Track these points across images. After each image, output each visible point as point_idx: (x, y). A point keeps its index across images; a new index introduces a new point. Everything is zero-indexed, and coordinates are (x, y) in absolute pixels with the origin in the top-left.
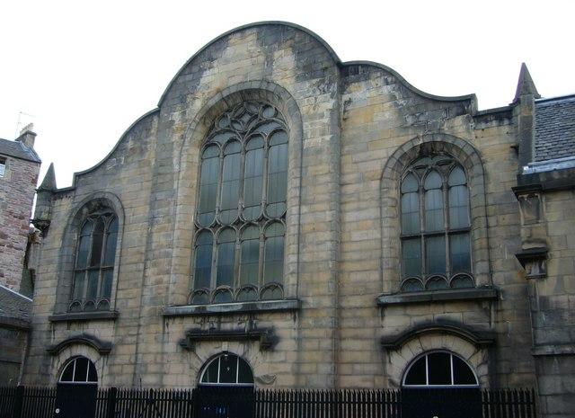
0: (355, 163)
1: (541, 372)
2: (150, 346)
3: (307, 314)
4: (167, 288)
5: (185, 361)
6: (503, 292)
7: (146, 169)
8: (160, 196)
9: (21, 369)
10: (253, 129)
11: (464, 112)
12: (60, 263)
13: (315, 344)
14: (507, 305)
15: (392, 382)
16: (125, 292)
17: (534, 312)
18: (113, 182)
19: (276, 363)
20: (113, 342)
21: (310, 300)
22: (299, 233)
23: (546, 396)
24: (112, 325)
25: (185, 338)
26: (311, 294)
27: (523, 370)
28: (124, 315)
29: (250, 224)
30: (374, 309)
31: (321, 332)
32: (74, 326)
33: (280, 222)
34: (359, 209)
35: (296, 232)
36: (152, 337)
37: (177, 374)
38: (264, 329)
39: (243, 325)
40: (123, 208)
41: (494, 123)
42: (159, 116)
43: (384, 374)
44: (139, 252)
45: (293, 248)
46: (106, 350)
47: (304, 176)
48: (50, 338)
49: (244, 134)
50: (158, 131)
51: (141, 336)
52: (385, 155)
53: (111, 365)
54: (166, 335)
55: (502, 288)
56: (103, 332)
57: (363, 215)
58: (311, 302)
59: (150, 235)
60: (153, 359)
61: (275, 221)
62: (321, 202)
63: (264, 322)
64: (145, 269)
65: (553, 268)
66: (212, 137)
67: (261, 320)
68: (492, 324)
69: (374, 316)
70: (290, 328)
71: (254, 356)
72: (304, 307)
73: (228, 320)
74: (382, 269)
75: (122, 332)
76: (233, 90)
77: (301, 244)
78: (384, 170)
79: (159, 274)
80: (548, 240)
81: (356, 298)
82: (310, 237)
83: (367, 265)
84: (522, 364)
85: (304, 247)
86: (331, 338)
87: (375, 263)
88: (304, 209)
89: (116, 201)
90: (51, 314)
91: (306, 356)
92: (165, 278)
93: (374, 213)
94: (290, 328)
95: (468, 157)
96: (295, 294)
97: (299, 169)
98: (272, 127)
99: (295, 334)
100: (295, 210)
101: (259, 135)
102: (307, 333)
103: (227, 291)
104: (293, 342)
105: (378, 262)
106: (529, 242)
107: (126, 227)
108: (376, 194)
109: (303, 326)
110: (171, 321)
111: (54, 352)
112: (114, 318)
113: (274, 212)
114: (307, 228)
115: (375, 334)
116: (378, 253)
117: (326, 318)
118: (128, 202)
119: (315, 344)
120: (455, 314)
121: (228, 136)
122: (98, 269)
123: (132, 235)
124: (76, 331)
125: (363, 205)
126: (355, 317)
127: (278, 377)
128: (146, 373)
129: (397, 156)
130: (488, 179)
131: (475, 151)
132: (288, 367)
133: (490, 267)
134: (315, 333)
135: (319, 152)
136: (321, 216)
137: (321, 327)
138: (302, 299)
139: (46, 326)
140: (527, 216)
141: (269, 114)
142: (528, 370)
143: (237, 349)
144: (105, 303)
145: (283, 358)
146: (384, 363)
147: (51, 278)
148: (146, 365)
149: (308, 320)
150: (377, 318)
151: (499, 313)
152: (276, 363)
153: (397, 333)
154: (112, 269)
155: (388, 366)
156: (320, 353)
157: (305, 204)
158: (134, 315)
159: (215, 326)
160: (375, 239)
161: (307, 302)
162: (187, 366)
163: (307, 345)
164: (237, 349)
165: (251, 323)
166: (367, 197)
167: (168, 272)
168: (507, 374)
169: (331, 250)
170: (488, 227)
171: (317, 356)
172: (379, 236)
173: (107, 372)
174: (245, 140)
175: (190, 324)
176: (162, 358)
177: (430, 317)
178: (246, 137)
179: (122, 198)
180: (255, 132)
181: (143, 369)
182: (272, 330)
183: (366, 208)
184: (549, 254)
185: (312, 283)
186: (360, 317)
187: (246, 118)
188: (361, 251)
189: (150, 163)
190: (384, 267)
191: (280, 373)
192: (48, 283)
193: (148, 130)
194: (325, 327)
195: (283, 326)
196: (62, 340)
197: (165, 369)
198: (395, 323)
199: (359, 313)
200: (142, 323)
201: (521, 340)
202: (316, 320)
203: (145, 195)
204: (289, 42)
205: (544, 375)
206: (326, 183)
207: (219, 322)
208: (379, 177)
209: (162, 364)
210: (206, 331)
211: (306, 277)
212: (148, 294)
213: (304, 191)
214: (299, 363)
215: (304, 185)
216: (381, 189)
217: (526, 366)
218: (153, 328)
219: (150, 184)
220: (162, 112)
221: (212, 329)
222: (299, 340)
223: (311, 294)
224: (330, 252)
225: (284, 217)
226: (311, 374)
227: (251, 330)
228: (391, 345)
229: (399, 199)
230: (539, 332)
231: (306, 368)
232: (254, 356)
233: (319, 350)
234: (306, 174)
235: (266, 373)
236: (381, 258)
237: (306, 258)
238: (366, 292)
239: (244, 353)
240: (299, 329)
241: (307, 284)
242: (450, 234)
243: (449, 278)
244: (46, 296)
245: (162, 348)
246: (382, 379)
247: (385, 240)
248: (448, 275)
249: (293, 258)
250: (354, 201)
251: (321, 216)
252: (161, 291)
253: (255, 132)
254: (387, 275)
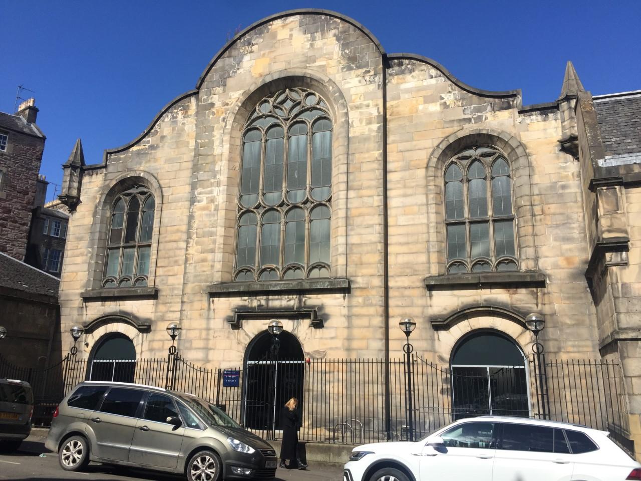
0: (401, 152)
1: (626, 355)
3: (355, 293)
4: (212, 266)
5: (232, 336)
6: (549, 276)
7: (184, 150)
8: (202, 175)
9: (50, 345)
10: (296, 116)
11: (509, 107)
12: (92, 240)
13: (364, 322)
14: (552, 287)
15: (442, 359)
16: (165, 269)
17: (615, 298)
18: (149, 161)
19: (326, 339)
20: (153, 318)
21: (359, 279)
22: (347, 217)
23: (631, 377)
24: (151, 302)
25: (232, 314)
26: (360, 274)
27: (571, 349)
28: (164, 292)
29: (295, 207)
30: (421, 289)
31: (372, 310)
32: (108, 303)
33: (326, 205)
34: (405, 196)
35: (344, 215)
36: (196, 314)
37: (224, 350)
38: (314, 307)
39: (292, 303)
40: (160, 187)
41: (539, 117)
42: (197, 99)
43: (433, 351)
44: (178, 231)
45: (342, 230)
46: (145, 328)
47: (350, 162)
48: (82, 315)
49: (287, 119)
50: (197, 113)
51: (184, 312)
52: (431, 146)
53: (150, 341)
54: (212, 312)
55: (548, 272)
56: (141, 308)
57: (409, 201)
58: (360, 281)
59: (191, 217)
60: (198, 335)
61: (321, 204)
62: (369, 187)
63: (313, 300)
64: (187, 247)
65: (633, 256)
66: (251, 123)
67: (310, 298)
68: (540, 305)
69: (424, 296)
70: (340, 306)
71: (302, 330)
72: (352, 286)
73: (276, 297)
74: (429, 252)
75: (162, 308)
76: (276, 77)
77: (349, 228)
78: (430, 159)
79: (202, 252)
80: (629, 230)
81: (403, 278)
82: (358, 221)
83: (414, 248)
84: (570, 343)
85: (352, 230)
86: (382, 316)
87: (421, 247)
88: (352, 194)
89: (153, 180)
90: (83, 291)
91: (356, 332)
92: (210, 256)
93: (422, 199)
94: (340, 306)
95: (513, 149)
96: (345, 275)
97: (346, 156)
98: (317, 114)
99: (345, 311)
100: (342, 194)
101: (303, 122)
102: (355, 310)
103: (273, 270)
104: (344, 319)
105: (425, 245)
106: (609, 231)
107: (164, 206)
108: (423, 182)
109: (354, 304)
110: (216, 299)
111: (89, 328)
112: (154, 295)
113: (319, 195)
114: (353, 212)
115: (423, 312)
116: (425, 236)
117: (376, 297)
118: (167, 181)
119: (364, 322)
121: (271, 121)
123: (170, 217)
124: (111, 307)
125: (409, 191)
126: (403, 296)
127: (328, 352)
128: (190, 349)
129: (443, 146)
130: (533, 170)
131: (521, 144)
132: (339, 343)
133: (536, 252)
134: (364, 311)
135: (366, 139)
136: (369, 201)
137: (371, 305)
138: (352, 279)
139: (77, 301)
140: (606, 206)
141: (311, 101)
142: (575, 349)
143: (287, 325)
144: (141, 279)
145: (333, 335)
146: (433, 339)
147: (82, 254)
148: (191, 341)
149: (358, 298)
150: (424, 298)
151: (546, 296)
152: (326, 339)
153: (445, 312)
154: (150, 246)
155: (437, 342)
156: (371, 329)
157: (352, 189)
158: (176, 292)
159: (263, 302)
160: (422, 224)
161: (356, 282)
162: (235, 342)
163: (356, 322)
164: (287, 325)
165: (300, 300)
166: (413, 184)
167: (212, 251)
168: (555, 353)
169: (380, 233)
170: (533, 215)
171: (368, 333)
172: (425, 221)
173: (147, 348)
174: (288, 125)
175: (237, 301)
176: (208, 334)
177: (478, 298)
178: (289, 123)
179: (159, 178)
180: (298, 119)
181: (187, 345)
182: (321, 308)
183: (411, 195)
184: (629, 243)
185: (356, 265)
186: (409, 297)
187: (289, 104)
188: (408, 234)
189: (188, 143)
190: (431, 250)
191: (331, 349)
192: (79, 260)
193: (186, 109)
194: (375, 305)
196: (95, 317)
197: (211, 345)
199: (407, 292)
200: (185, 300)
201: (568, 322)
202: (366, 298)
203: (186, 175)
204: (334, 31)
205: (628, 357)
206: (373, 170)
207: (267, 300)
208: (425, 166)
209: (207, 339)
210: (255, 308)
211: (354, 258)
212: (190, 269)
213: (351, 177)
214: (349, 339)
215: (350, 171)
216: (427, 177)
217: (573, 346)
218: (197, 305)
219: (190, 165)
220: (201, 95)
221: (260, 306)
222: (349, 317)
223: (360, 274)
224: (378, 235)
225: (329, 200)
226: (361, 349)
227: (300, 307)
228: (441, 324)
229: (442, 185)
230: (622, 316)
231: (355, 344)
232: (302, 330)
233: (368, 327)
234: (353, 160)
235: (317, 348)
236: (428, 241)
237: (354, 239)
238: (414, 273)
239: (294, 330)
240: (350, 307)
241: (356, 265)
242: (494, 221)
243: (494, 261)
244: (76, 272)
245: (208, 324)
246: (431, 354)
247: (431, 225)
248: (493, 259)
249: (342, 240)
250: (399, 188)
251: (369, 201)
252: (205, 269)
253: (298, 119)
254: (434, 257)
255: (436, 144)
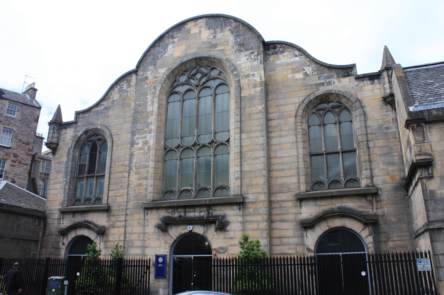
0: (277, 106)
1: (434, 239)
2: (135, 228)
4: (146, 189)
6: (380, 189)
8: (139, 126)
9: (39, 245)
10: (204, 83)
11: (349, 75)
12: (67, 172)
13: (255, 226)
14: (384, 196)
15: (309, 250)
16: (115, 192)
20: (107, 226)
21: (250, 196)
22: (241, 152)
23: (438, 255)
25: (161, 223)
26: (251, 192)
27: (395, 239)
30: (294, 202)
31: (259, 218)
32: (77, 215)
33: (225, 144)
36: (136, 223)
38: (218, 216)
39: (202, 214)
40: (111, 135)
41: (369, 82)
43: (303, 244)
44: (123, 165)
46: (102, 232)
48: (60, 223)
52: (298, 101)
53: (105, 242)
54: (146, 221)
56: (100, 220)
58: (251, 198)
59: (132, 155)
60: (137, 237)
62: (256, 131)
63: (218, 212)
66: (173, 89)
67: (215, 210)
68: (375, 210)
69: (296, 206)
70: (237, 215)
72: (247, 201)
73: (192, 210)
74: (299, 175)
76: (190, 58)
77: (243, 160)
78: (297, 111)
79: (139, 180)
82: (248, 155)
84: (395, 234)
86: (267, 221)
87: (294, 172)
89: (106, 131)
90: (60, 207)
92: (144, 182)
93: (293, 139)
95: (353, 103)
96: (240, 193)
97: (239, 109)
98: (217, 82)
99: (240, 219)
103: (188, 190)
105: (296, 170)
108: (293, 126)
110: (149, 212)
112: (107, 210)
113: (221, 138)
115: (296, 217)
116: (295, 165)
117: (263, 208)
119: (255, 226)
120: (350, 204)
121: (186, 87)
122: (93, 177)
123: (117, 154)
124: (79, 219)
127: (229, 248)
128: (132, 247)
129: (306, 102)
130: (367, 118)
131: (358, 100)
132: (236, 242)
133: (372, 173)
137: (259, 214)
138: (245, 196)
139: (56, 215)
141: (214, 73)
142: (398, 239)
143: (199, 230)
144: (99, 199)
146: (302, 237)
147: (60, 182)
148: (132, 242)
151: (379, 203)
153: (310, 217)
155: (305, 238)
156: (259, 231)
158: (122, 207)
159: (182, 214)
160: (293, 156)
161: (249, 198)
162: (163, 242)
164: (199, 230)
165: (209, 212)
166: (287, 128)
167: (146, 178)
169: (264, 163)
170: (368, 148)
172: (296, 154)
173: (103, 247)
175: (163, 213)
176: (144, 237)
179: (110, 129)
180: (205, 85)
181: (130, 244)
182: (224, 216)
184: (433, 162)
185: (248, 186)
187: (199, 76)
189: (130, 104)
190: (300, 174)
191: (231, 245)
192: (58, 186)
193: (129, 82)
194: (262, 214)
195: (232, 215)
198: (309, 211)
200: (128, 213)
201: (393, 220)
203: (128, 126)
204: (229, 28)
205: (436, 241)
206: (259, 119)
207: (185, 212)
208: (294, 115)
209: (144, 240)
210: (176, 218)
212: (131, 192)
215: (242, 120)
216: (296, 123)
217: (397, 236)
218: (136, 216)
219: (131, 119)
221: (180, 216)
222: (243, 223)
223: (251, 192)
224: (263, 164)
225: (228, 141)
227: (208, 217)
229: (307, 129)
233: (258, 229)
235: (221, 245)
236: (298, 168)
239: (204, 233)
241: (248, 186)
242: (343, 152)
245: (144, 229)
247: (300, 156)
248: (343, 179)
252: (141, 191)
253: (205, 85)
254: (302, 179)
255: (301, 100)
